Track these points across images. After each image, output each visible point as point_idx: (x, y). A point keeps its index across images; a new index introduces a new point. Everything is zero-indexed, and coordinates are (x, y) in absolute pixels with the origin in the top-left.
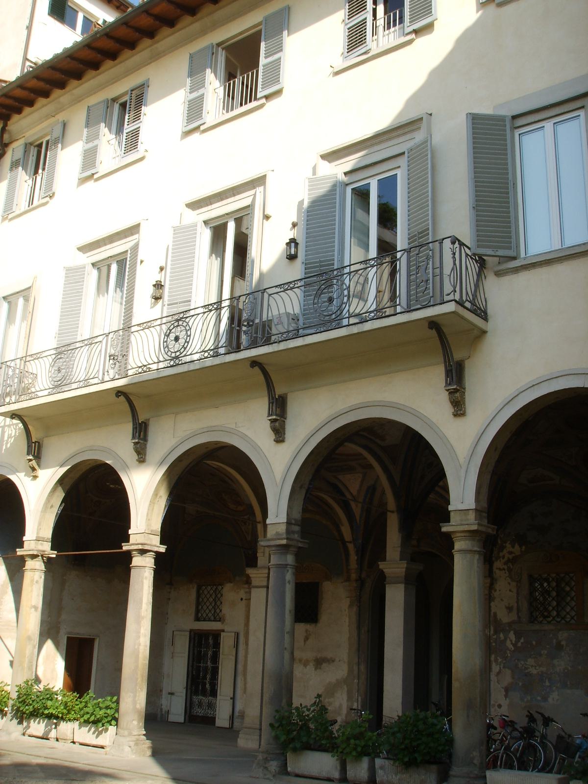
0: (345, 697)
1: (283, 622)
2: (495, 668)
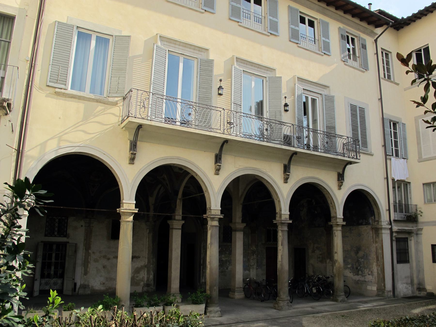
0: (146, 274)
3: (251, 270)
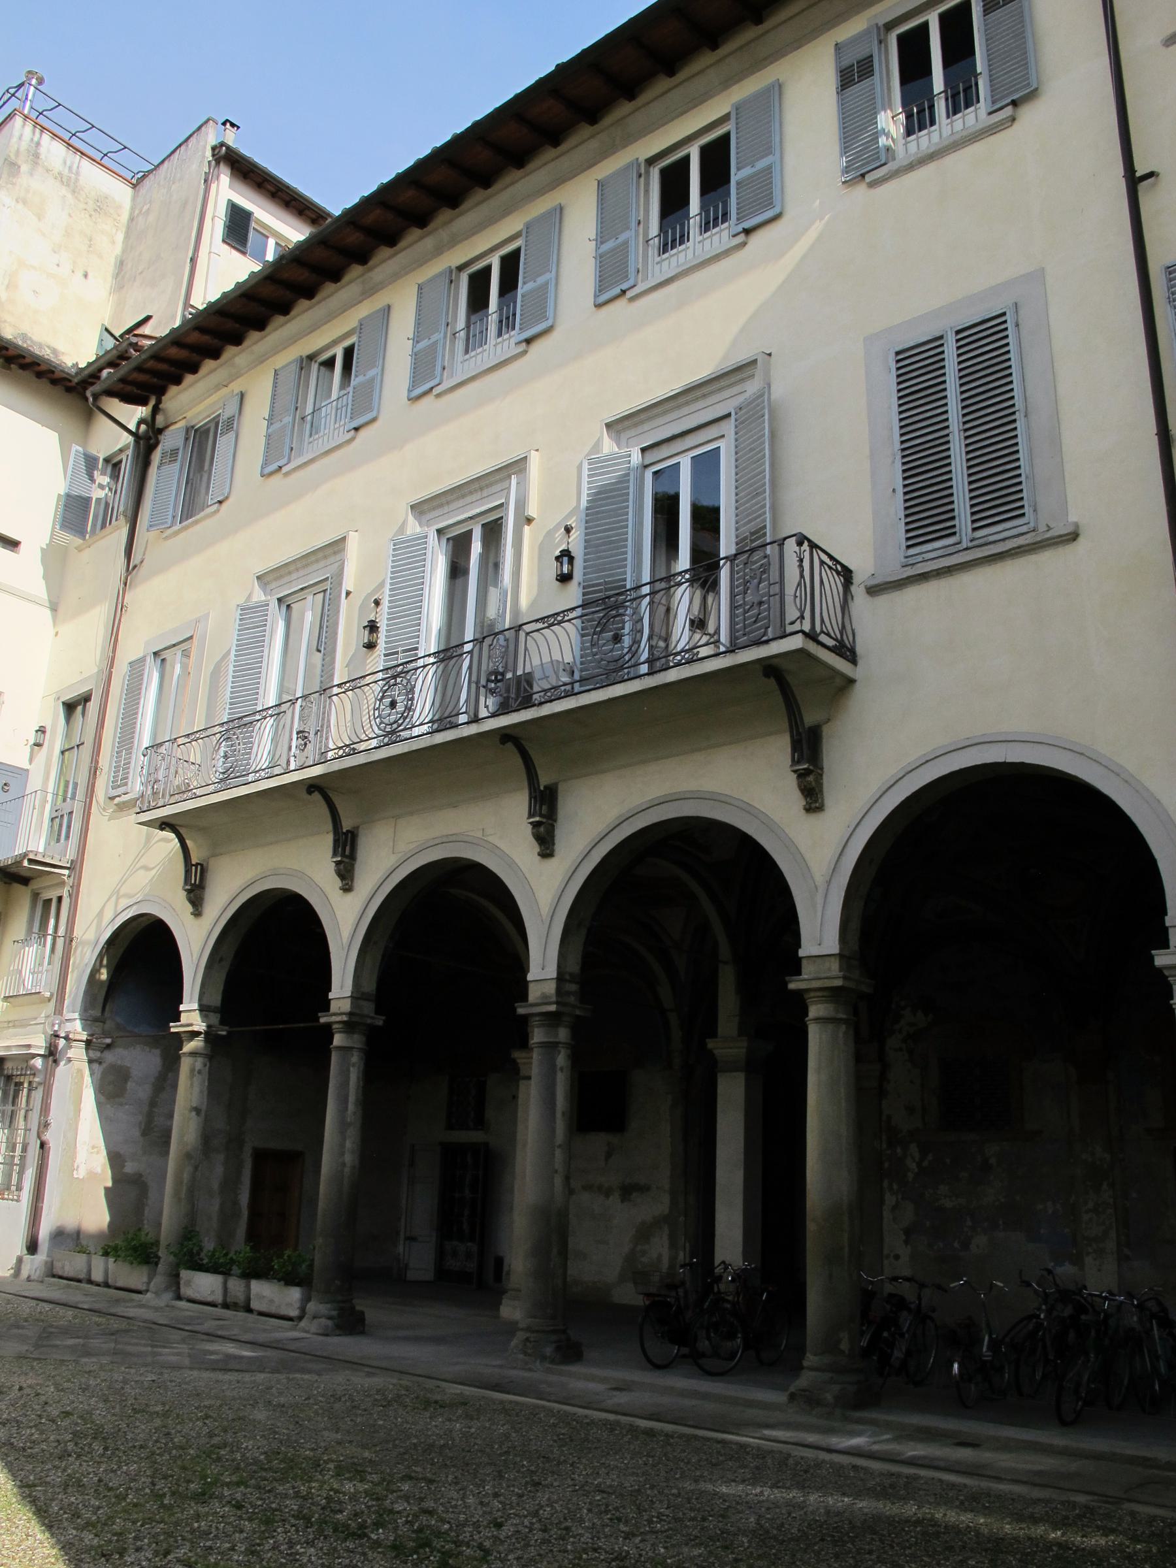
0: (666, 1242)
1: (553, 1131)
2: (890, 1200)
3: (1088, 1260)
